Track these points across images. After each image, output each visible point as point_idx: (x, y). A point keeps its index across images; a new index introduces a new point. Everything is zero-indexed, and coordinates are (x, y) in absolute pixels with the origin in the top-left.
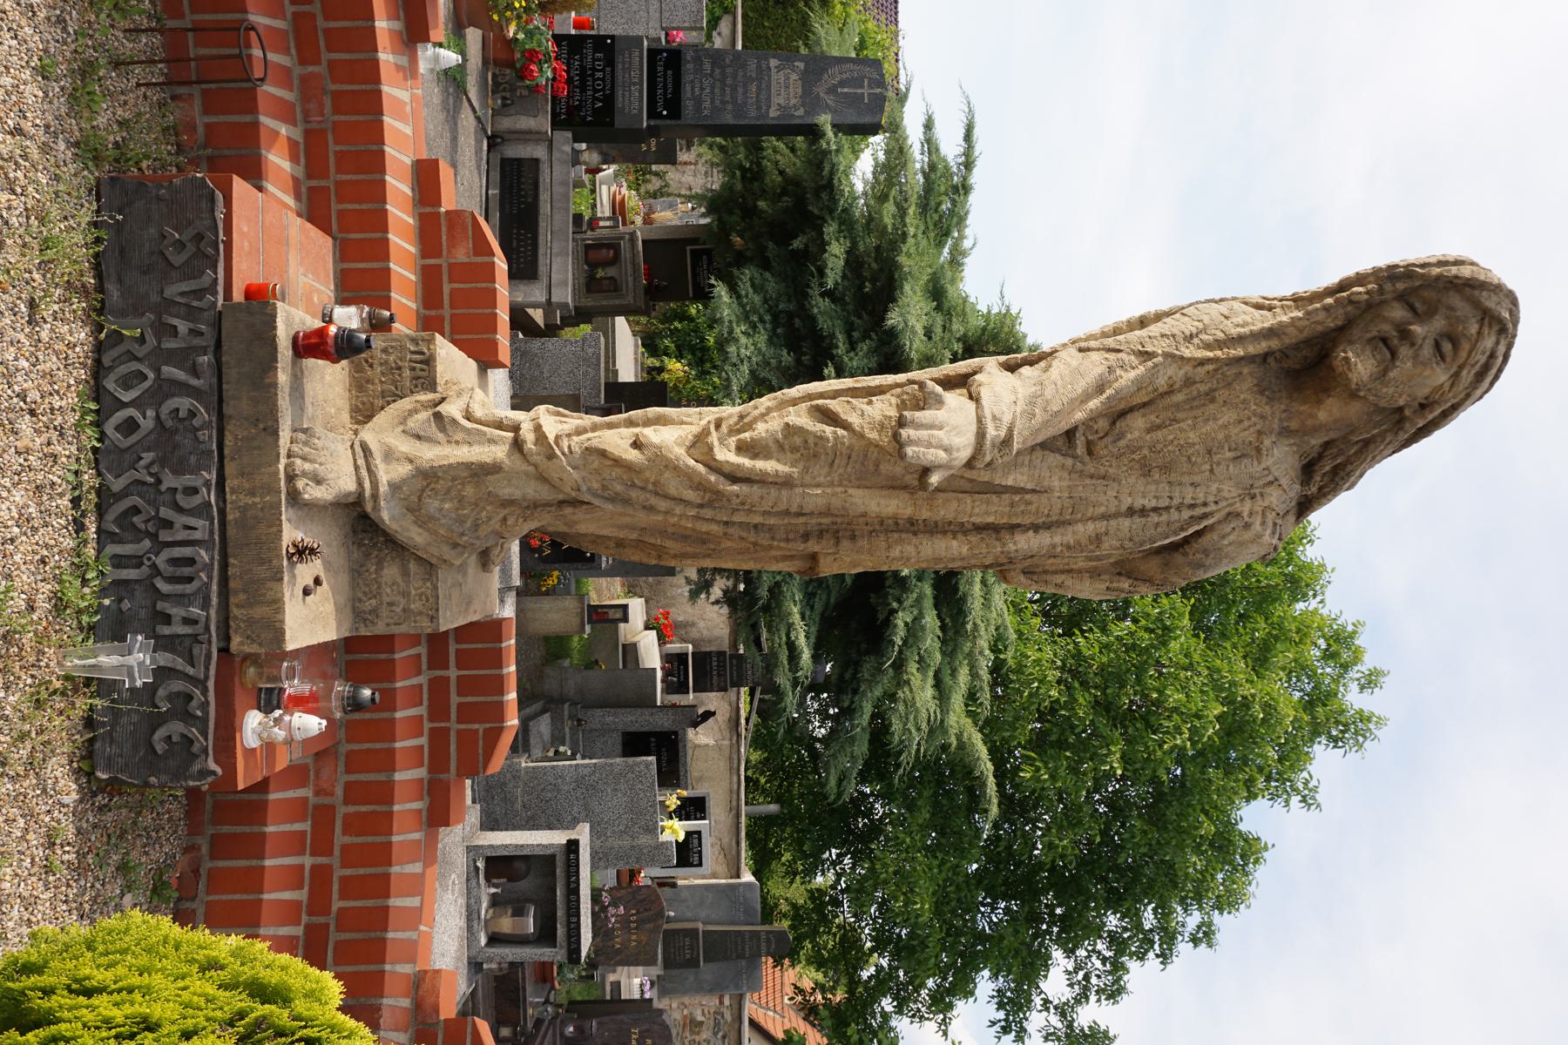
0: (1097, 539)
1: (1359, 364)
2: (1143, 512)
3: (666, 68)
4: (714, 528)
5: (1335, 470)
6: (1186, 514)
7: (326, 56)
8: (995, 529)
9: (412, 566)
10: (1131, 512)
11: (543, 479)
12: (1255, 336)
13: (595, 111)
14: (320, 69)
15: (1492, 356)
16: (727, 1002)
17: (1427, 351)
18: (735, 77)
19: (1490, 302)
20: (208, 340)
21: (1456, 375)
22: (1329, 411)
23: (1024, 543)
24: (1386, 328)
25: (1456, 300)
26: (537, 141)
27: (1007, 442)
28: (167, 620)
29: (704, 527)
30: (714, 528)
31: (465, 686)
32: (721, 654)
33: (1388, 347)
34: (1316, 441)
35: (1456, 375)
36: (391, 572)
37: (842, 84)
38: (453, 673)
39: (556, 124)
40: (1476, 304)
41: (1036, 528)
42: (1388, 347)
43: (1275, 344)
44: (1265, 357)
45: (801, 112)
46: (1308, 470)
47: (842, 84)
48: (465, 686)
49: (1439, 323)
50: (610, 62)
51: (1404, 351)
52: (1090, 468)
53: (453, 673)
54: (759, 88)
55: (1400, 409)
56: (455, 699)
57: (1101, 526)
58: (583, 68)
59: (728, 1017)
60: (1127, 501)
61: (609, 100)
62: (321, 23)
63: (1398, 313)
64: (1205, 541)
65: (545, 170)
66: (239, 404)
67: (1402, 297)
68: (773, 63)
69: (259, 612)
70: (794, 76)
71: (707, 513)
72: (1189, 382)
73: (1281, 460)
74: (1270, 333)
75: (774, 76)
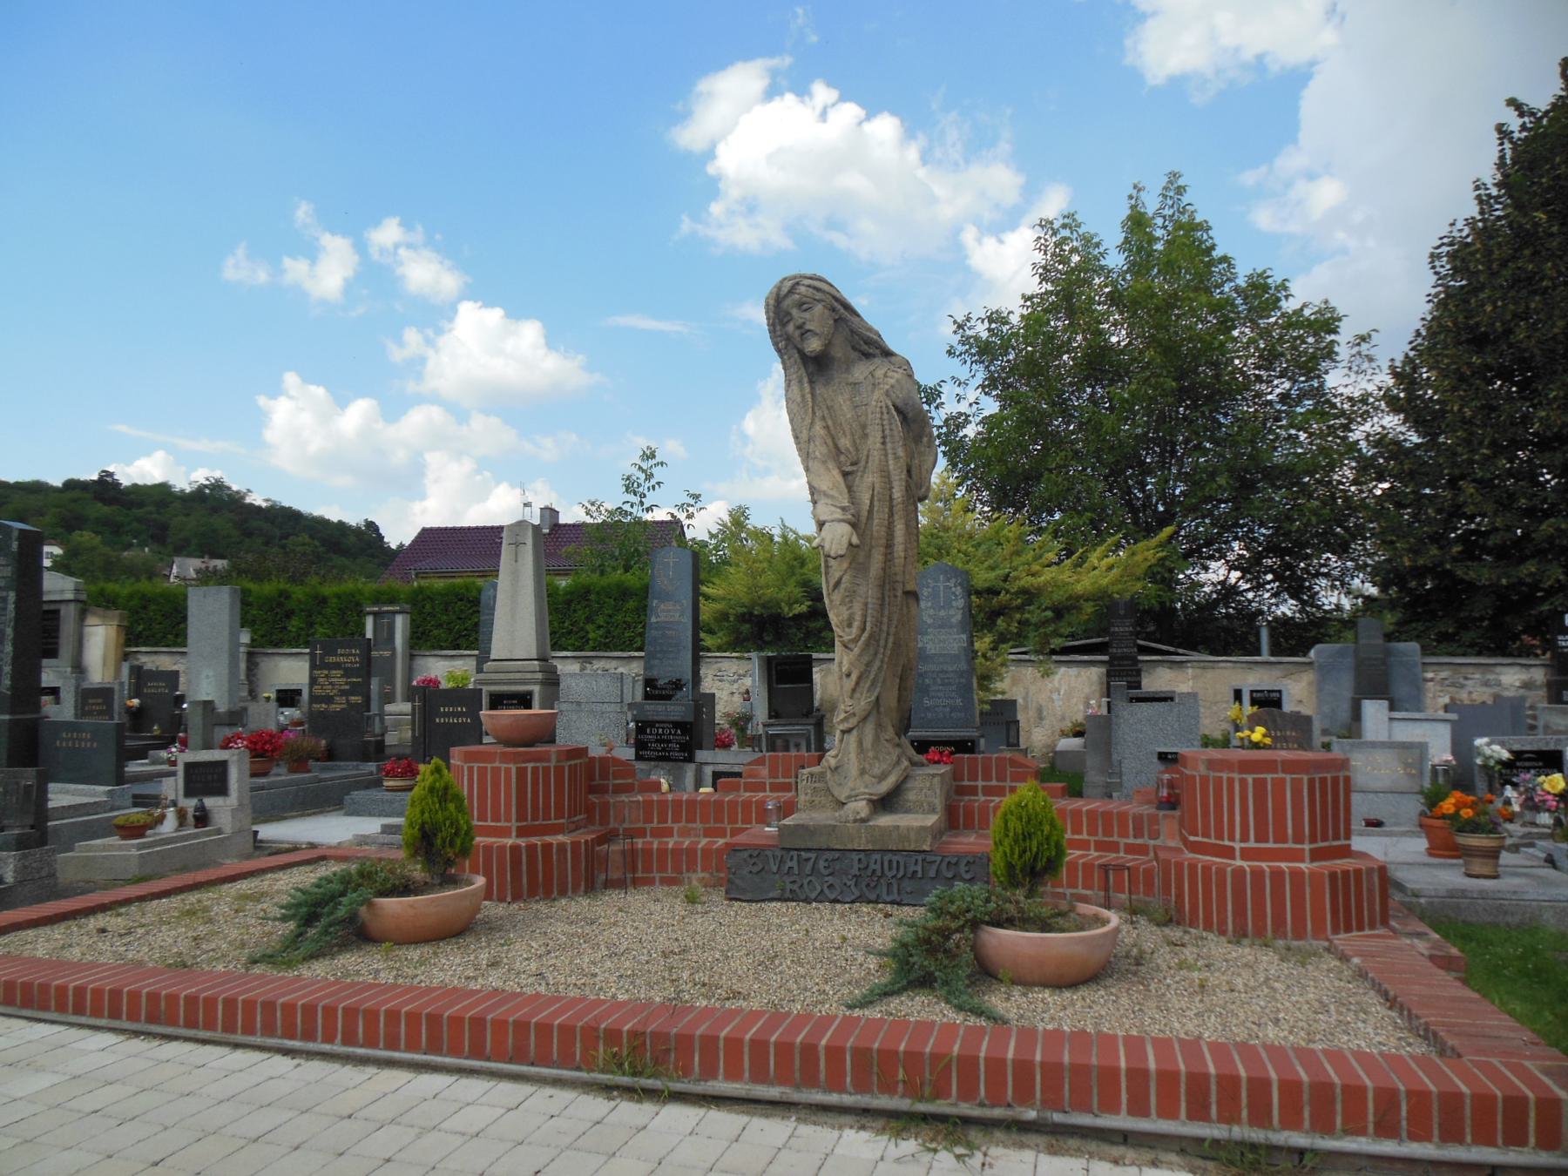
0: (896, 458)
1: (814, 345)
2: (884, 437)
4: (891, 640)
6: (886, 416)
7: (669, 824)
8: (891, 508)
9: (909, 785)
10: (884, 443)
11: (865, 719)
12: (802, 389)
14: (676, 827)
16: (1430, 675)
17: (807, 315)
19: (785, 290)
20: (795, 853)
22: (838, 352)
23: (898, 494)
24: (797, 333)
25: (787, 303)
27: (843, 509)
28: (915, 872)
29: (890, 645)
30: (891, 640)
31: (987, 777)
32: (1109, 674)
33: (804, 333)
34: (854, 355)
36: (911, 796)
38: (980, 783)
39: (690, 759)
40: (786, 296)
41: (891, 488)
42: (804, 333)
43: (806, 380)
44: (811, 382)
46: (867, 356)
48: (987, 777)
49: (795, 312)
50: (652, 724)
51: (808, 327)
52: (862, 463)
53: (980, 783)
55: (836, 321)
56: (994, 783)
57: (890, 457)
58: (657, 741)
59: (1444, 674)
60: (878, 445)
61: (676, 725)
62: (655, 825)
63: (791, 328)
66: (822, 842)
67: (784, 325)
68: (653, 620)
69: (912, 836)
71: (882, 642)
72: (823, 418)
73: (860, 371)
74: (800, 381)
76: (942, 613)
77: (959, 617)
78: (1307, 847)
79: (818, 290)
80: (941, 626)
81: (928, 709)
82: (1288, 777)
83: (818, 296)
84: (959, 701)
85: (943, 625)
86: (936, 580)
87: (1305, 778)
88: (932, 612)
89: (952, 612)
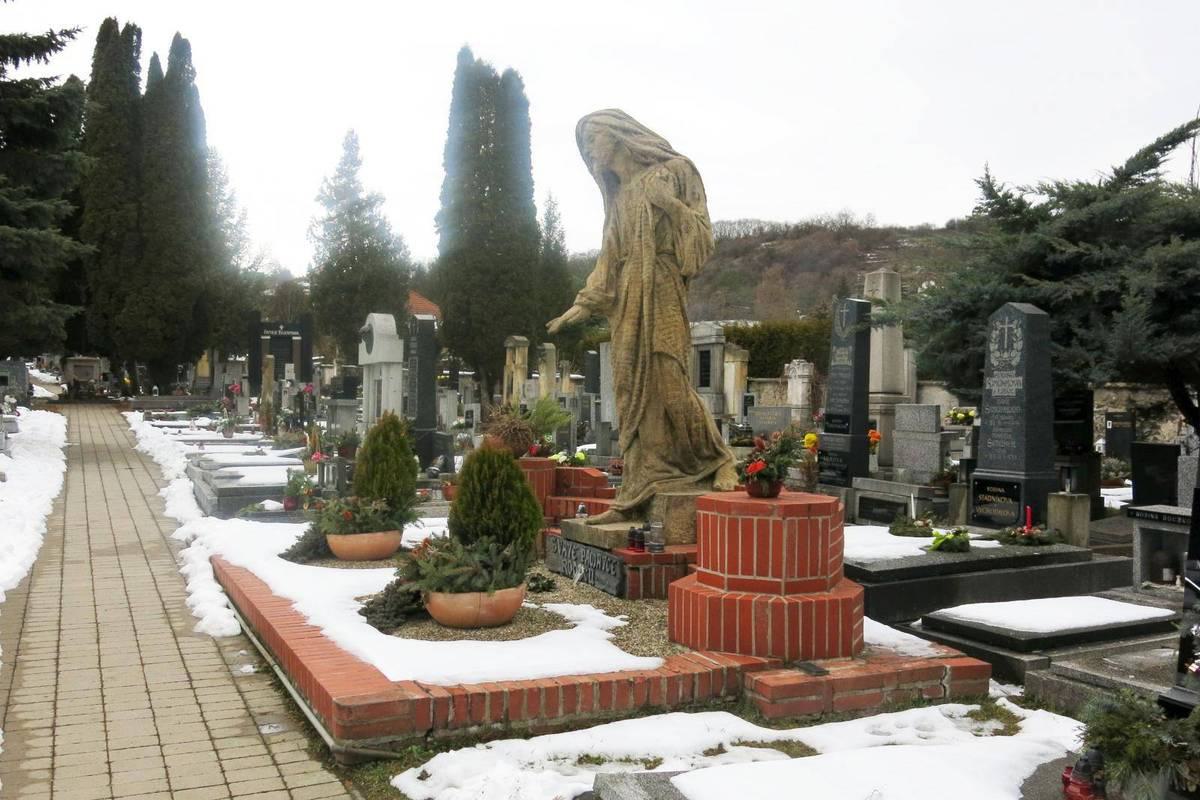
3: (831, 422)
5: (642, 155)
9: (655, 502)
13: (844, 462)
15: (593, 122)
18: (836, 385)
21: (599, 132)
26: (855, 496)
35: (599, 132)
37: (842, 325)
45: (851, 348)
46: (648, 165)
47: (842, 325)
54: (841, 371)
64: (655, 203)
65: (868, 495)
68: (833, 364)
70: (838, 352)
75: (837, 363)
76: (1006, 355)
77: (1018, 359)
78: (726, 576)
79: (597, 123)
80: (1004, 369)
81: (990, 449)
82: (719, 515)
83: (598, 128)
84: (1013, 443)
85: (1008, 366)
86: (1003, 322)
87: (727, 517)
88: (998, 354)
89: (1013, 354)
